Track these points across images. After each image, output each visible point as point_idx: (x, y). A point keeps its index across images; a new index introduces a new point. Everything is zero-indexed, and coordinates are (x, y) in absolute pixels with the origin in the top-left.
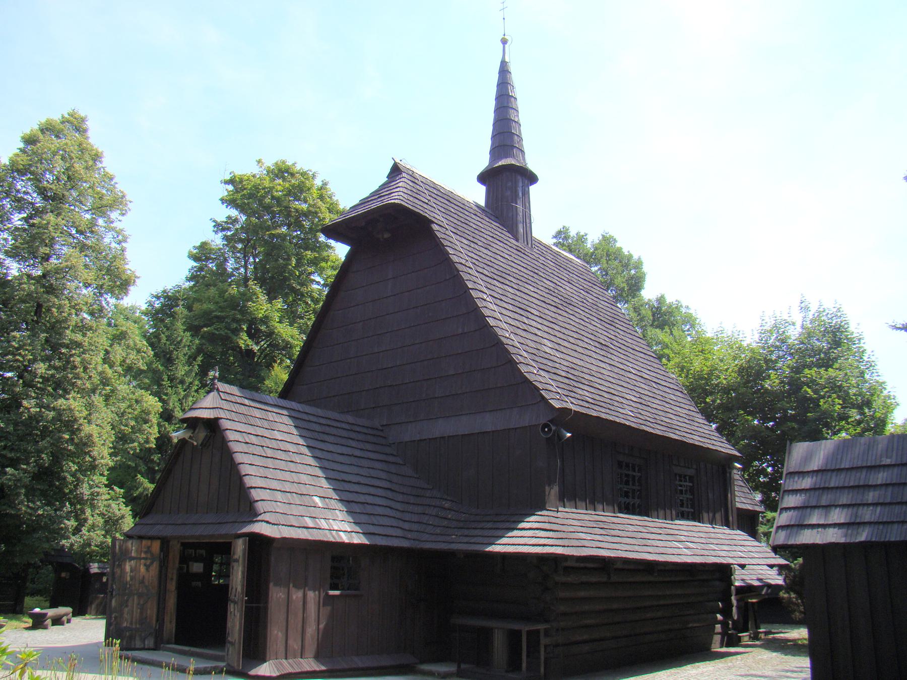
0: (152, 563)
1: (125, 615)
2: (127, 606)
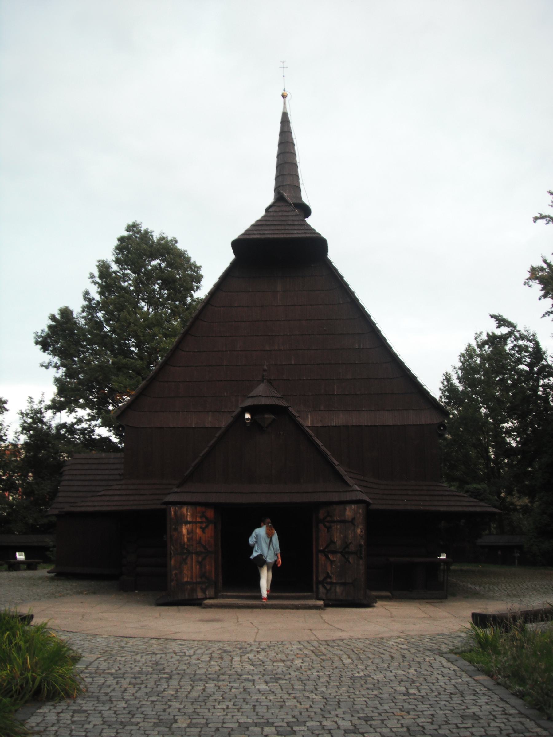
0: (207, 526)
1: (185, 572)
2: (186, 564)
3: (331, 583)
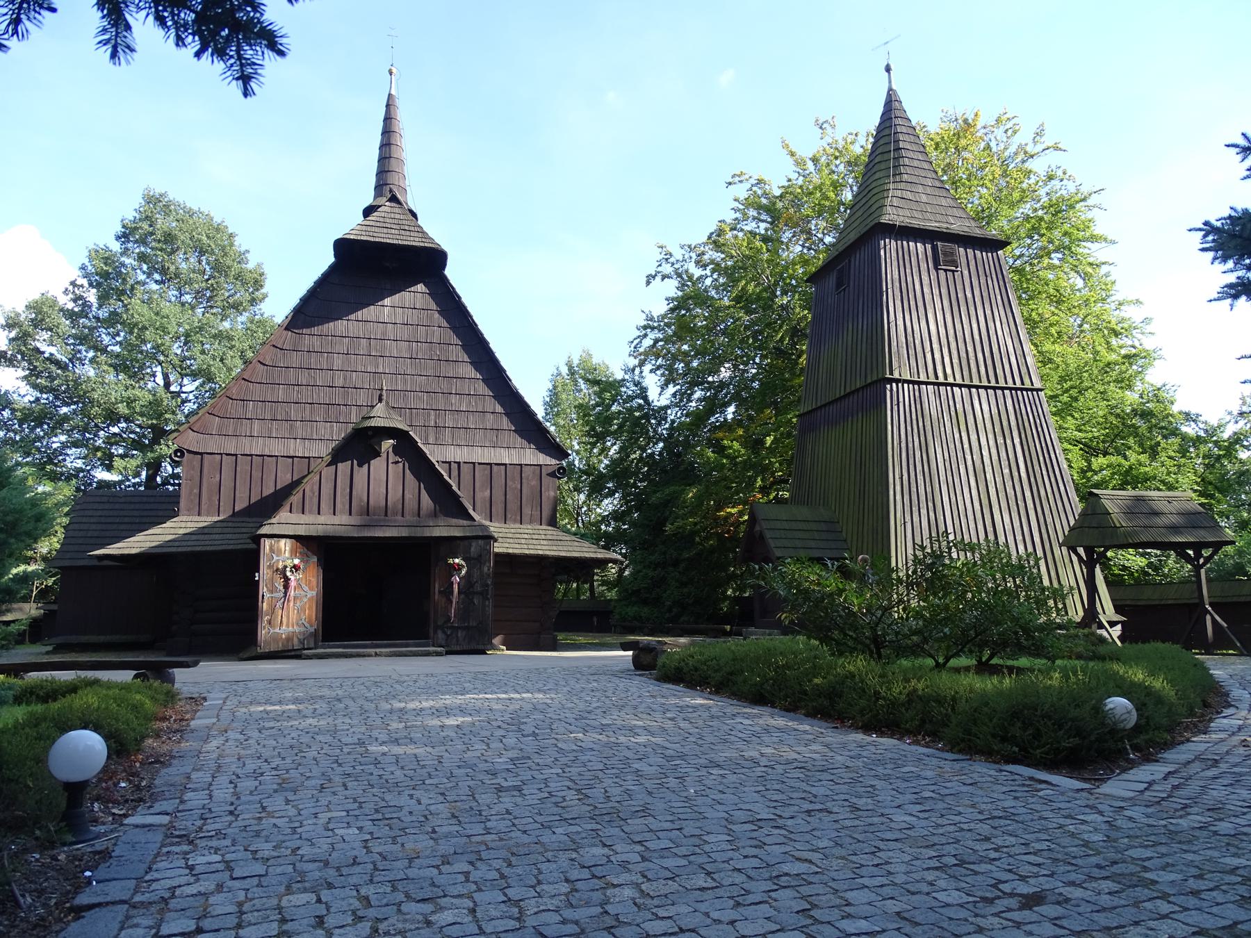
3: (452, 628)
